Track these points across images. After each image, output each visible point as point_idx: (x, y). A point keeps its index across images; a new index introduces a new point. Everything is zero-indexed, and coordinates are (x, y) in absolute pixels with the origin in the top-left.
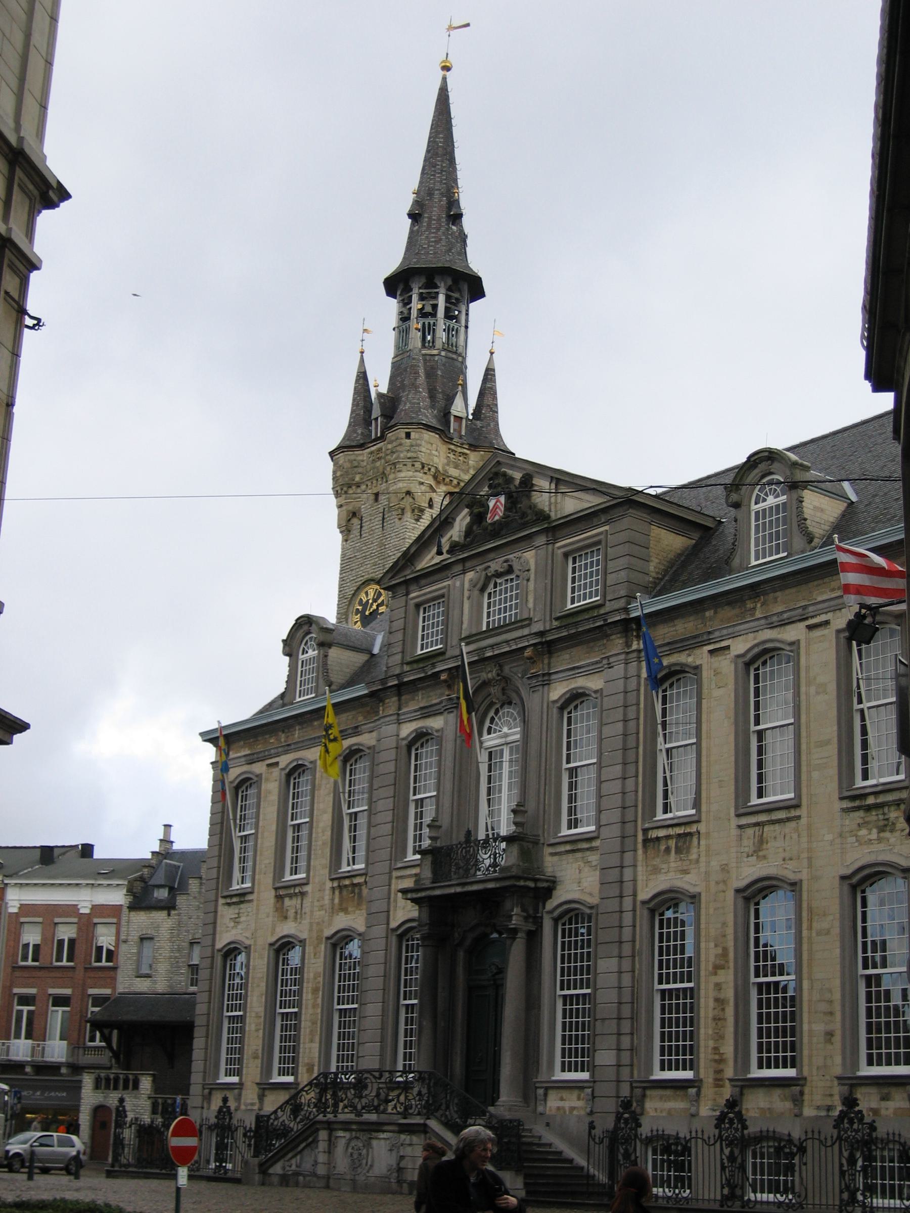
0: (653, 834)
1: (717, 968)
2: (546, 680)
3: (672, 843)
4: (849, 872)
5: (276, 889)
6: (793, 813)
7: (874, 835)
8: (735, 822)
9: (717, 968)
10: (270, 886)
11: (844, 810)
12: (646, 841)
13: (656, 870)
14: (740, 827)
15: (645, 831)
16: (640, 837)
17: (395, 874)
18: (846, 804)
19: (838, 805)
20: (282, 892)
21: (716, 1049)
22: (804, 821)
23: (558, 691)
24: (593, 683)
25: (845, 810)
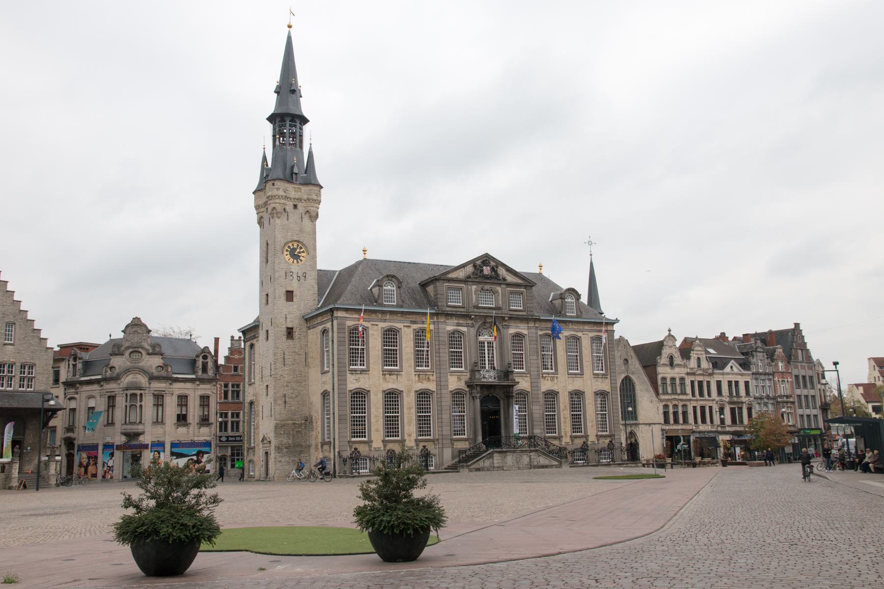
0: (544, 375)
1: (563, 410)
2: (508, 327)
3: (549, 378)
4: (596, 391)
5: (383, 371)
6: (582, 376)
7: (600, 384)
8: (567, 376)
9: (563, 410)
10: (381, 370)
11: (594, 377)
12: (542, 377)
13: (545, 384)
14: (568, 377)
15: (542, 374)
16: (541, 376)
17: (449, 374)
18: (594, 376)
19: (593, 376)
20: (384, 373)
21: (565, 429)
22: (584, 378)
23: (512, 331)
24: (525, 332)
25: (594, 377)
